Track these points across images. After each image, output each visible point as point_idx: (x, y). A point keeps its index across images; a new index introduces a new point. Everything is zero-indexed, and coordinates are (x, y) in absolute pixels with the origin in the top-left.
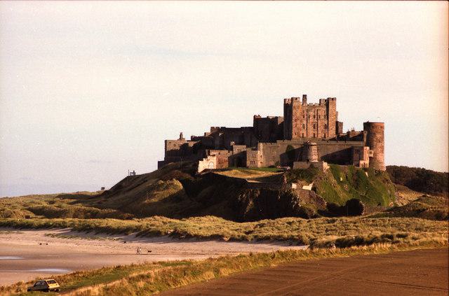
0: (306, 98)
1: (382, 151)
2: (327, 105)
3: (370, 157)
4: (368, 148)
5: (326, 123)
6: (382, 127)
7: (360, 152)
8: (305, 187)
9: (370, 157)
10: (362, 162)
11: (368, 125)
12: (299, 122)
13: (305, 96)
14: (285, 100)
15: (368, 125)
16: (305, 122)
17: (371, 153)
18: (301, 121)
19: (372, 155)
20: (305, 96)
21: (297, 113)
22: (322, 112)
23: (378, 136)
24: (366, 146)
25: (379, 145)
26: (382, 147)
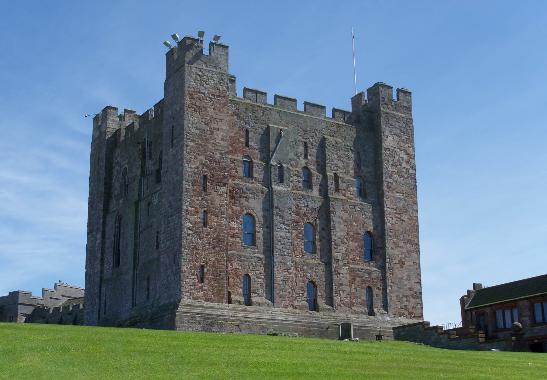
12: (219, 197)
18: (235, 195)
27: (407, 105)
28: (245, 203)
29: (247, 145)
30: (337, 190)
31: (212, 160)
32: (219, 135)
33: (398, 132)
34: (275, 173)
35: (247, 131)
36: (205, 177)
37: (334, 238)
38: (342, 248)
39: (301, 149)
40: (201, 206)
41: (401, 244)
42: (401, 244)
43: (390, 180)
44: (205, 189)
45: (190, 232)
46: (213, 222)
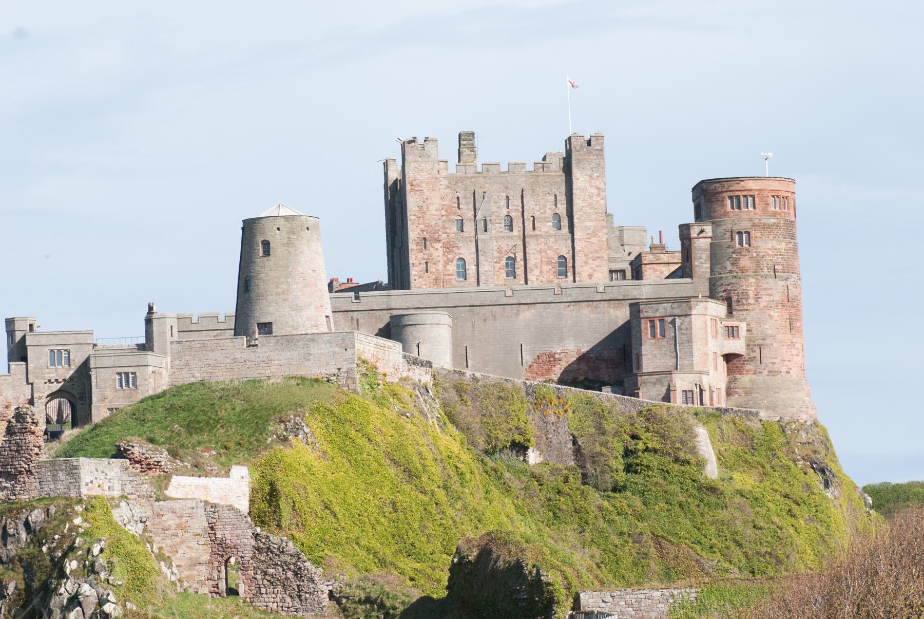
0: (472, 149)
1: (792, 324)
2: (567, 168)
3: (729, 358)
4: (718, 309)
5: (566, 251)
6: (783, 200)
7: (673, 323)
8: (183, 486)
9: (729, 358)
10: (681, 382)
11: (707, 196)
12: (437, 251)
13: (466, 140)
14: (386, 164)
15: (707, 196)
16: (468, 253)
17: (732, 332)
18: (449, 247)
19: (737, 346)
20: (466, 140)
21: (425, 209)
22: (544, 205)
23: (768, 246)
24: (712, 295)
25: (775, 289)
26: (790, 303)
27: (599, 148)
28: (457, 251)
29: (459, 208)
30: (534, 228)
31: (429, 226)
32: (433, 208)
33: (590, 172)
34: (481, 225)
35: (458, 198)
36: (425, 239)
37: (528, 265)
38: (537, 272)
39: (503, 202)
40: (423, 259)
41: (590, 261)
42: (590, 261)
43: (580, 213)
44: (425, 247)
45: (416, 278)
46: (432, 268)
